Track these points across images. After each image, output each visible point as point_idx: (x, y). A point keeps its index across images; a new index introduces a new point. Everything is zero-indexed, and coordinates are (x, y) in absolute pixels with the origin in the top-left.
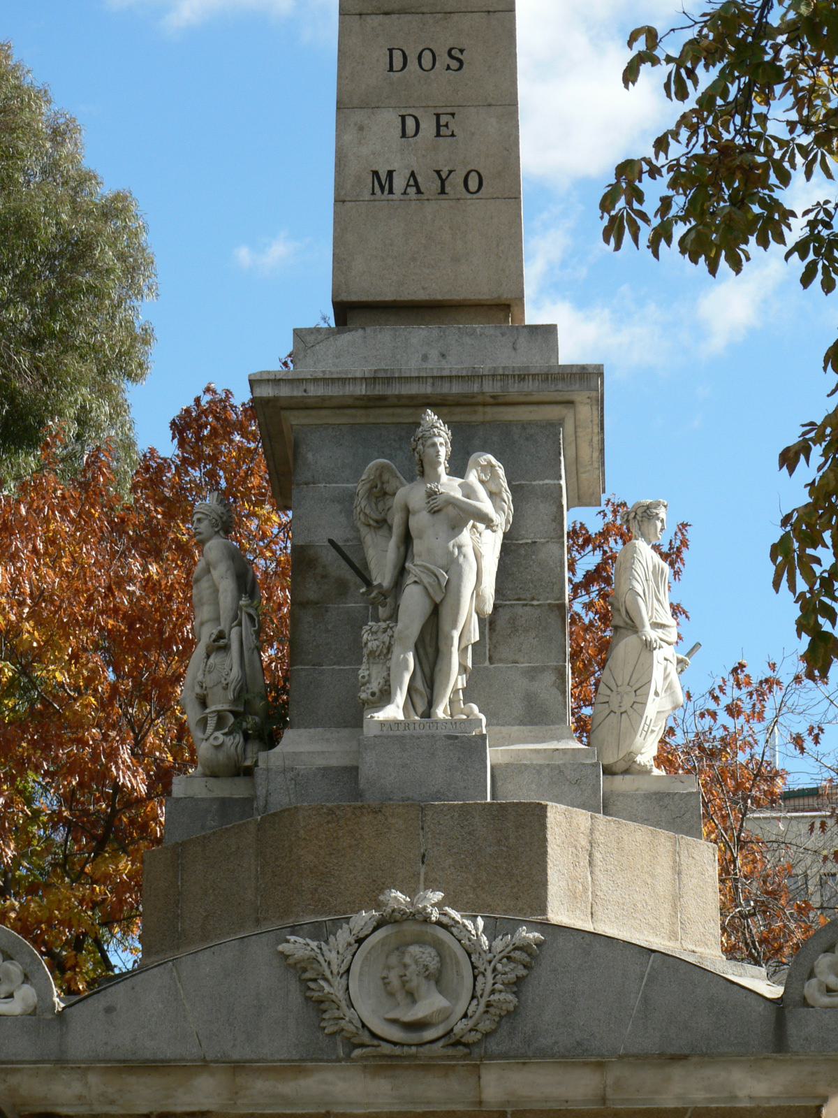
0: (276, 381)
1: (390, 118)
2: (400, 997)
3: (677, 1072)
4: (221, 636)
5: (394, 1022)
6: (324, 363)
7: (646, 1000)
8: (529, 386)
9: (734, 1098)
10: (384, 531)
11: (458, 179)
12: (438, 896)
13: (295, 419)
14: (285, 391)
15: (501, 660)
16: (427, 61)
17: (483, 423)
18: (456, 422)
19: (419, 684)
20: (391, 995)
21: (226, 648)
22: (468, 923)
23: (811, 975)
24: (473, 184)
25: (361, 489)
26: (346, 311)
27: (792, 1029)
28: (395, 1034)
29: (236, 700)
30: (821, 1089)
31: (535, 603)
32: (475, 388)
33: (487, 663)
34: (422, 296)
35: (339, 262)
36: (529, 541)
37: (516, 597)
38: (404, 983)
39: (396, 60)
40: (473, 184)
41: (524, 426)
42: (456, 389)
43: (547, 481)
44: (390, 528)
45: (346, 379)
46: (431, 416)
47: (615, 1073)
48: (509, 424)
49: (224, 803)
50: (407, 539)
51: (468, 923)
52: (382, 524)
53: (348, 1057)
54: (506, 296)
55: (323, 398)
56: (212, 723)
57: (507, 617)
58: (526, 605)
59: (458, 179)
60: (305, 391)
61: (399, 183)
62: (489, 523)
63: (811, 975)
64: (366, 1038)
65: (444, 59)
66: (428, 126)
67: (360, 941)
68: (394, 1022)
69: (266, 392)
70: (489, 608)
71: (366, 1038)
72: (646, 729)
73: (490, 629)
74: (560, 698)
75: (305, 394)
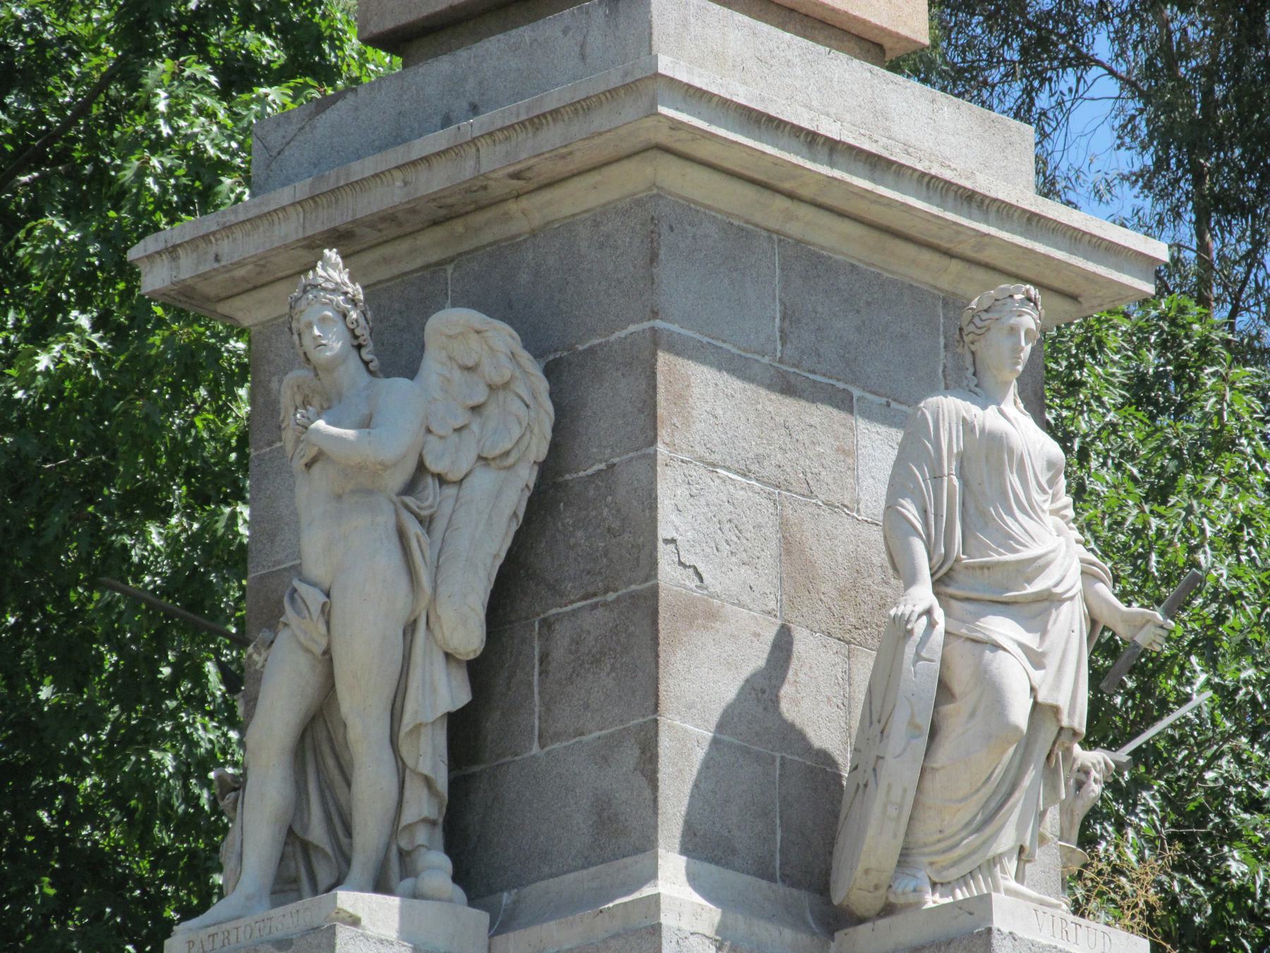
8: (552, 136)
15: (557, 736)
17: (534, 234)
18: (490, 244)
31: (611, 596)
32: (466, 170)
33: (535, 749)
36: (603, 466)
37: (582, 592)
41: (596, 218)
43: (632, 328)
45: (269, 213)
48: (569, 224)
55: (261, 262)
57: (566, 642)
58: (594, 607)
60: (217, 259)
72: (892, 812)
73: (540, 674)
74: (647, 793)
75: (216, 265)
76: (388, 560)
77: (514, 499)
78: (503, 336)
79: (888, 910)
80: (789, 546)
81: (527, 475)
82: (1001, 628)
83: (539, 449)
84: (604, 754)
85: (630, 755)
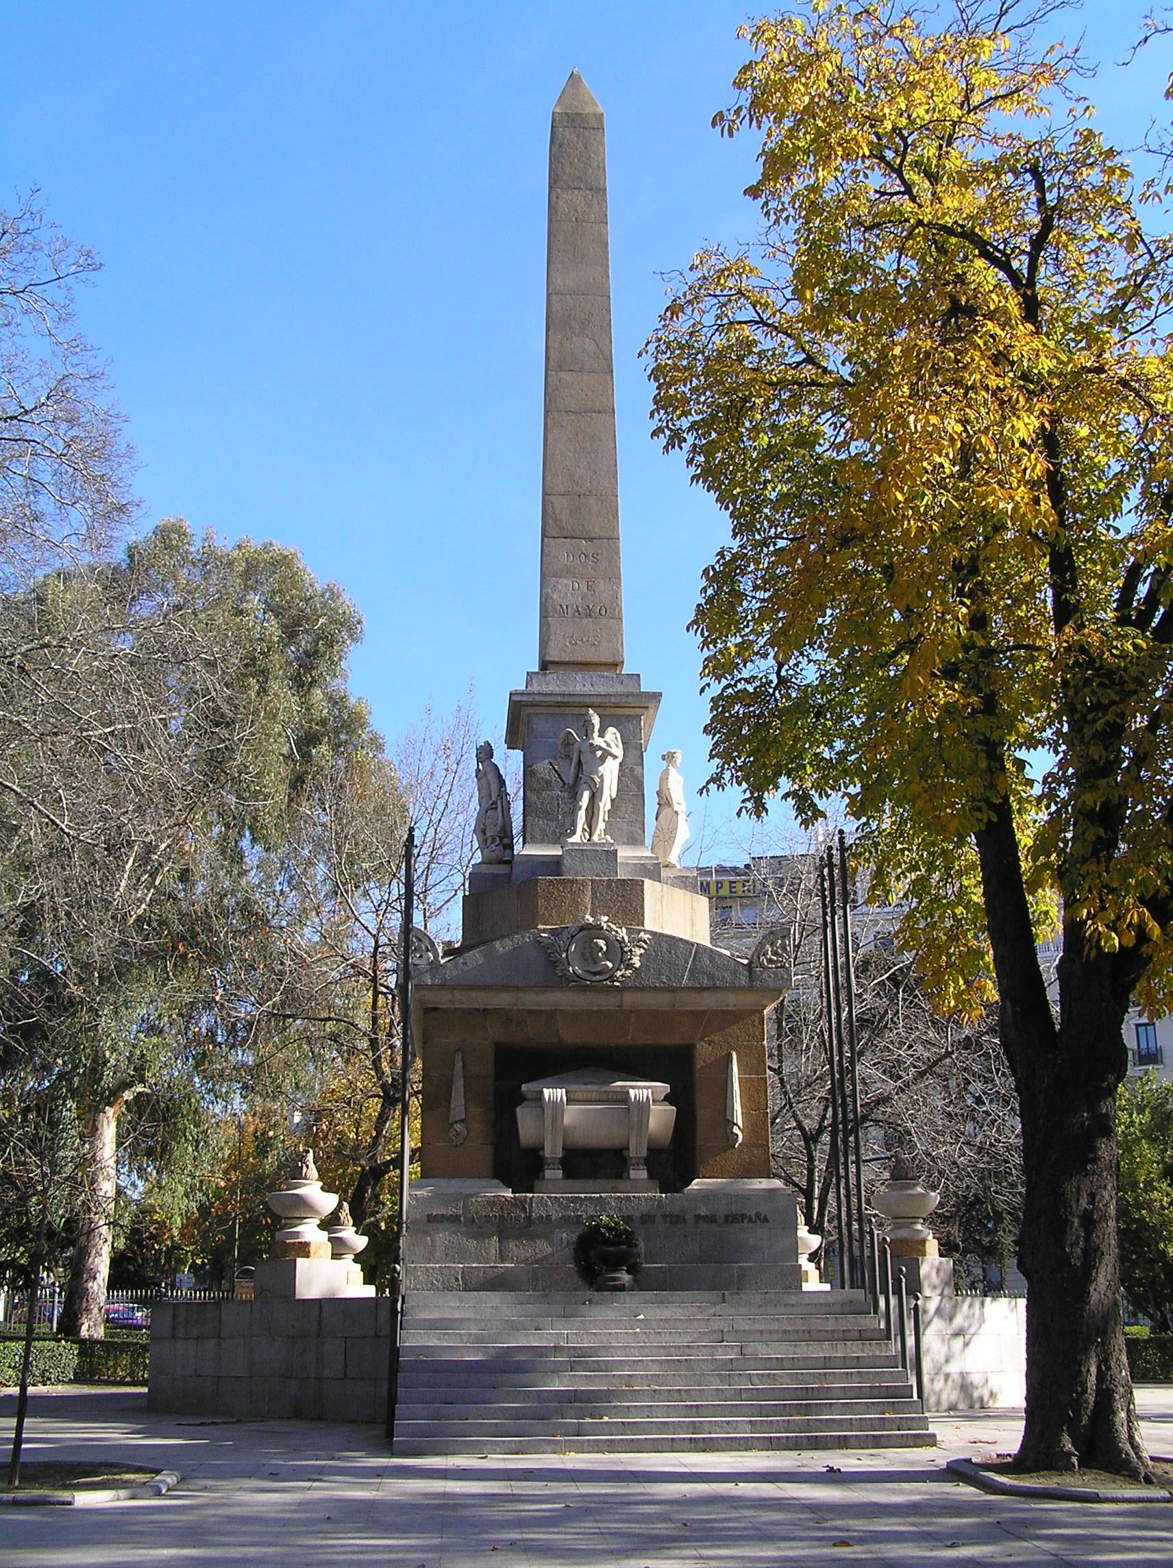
0: (522, 694)
2: (590, 961)
3: (706, 994)
4: (493, 803)
5: (588, 971)
6: (535, 688)
8: (630, 699)
10: (568, 760)
12: (605, 918)
13: (529, 710)
14: (524, 698)
19: (586, 827)
20: (586, 960)
21: (496, 808)
22: (619, 930)
25: (560, 742)
26: (545, 665)
28: (586, 976)
29: (499, 832)
30: (765, 1003)
34: (579, 659)
35: (544, 643)
38: (591, 955)
42: (599, 700)
44: (571, 759)
46: (591, 712)
47: (679, 995)
49: (494, 875)
50: (580, 763)
51: (619, 930)
52: (568, 757)
54: (618, 660)
56: (489, 840)
62: (615, 757)
64: (576, 979)
67: (573, 937)
68: (588, 971)
69: (515, 698)
70: (614, 796)
71: (576, 979)
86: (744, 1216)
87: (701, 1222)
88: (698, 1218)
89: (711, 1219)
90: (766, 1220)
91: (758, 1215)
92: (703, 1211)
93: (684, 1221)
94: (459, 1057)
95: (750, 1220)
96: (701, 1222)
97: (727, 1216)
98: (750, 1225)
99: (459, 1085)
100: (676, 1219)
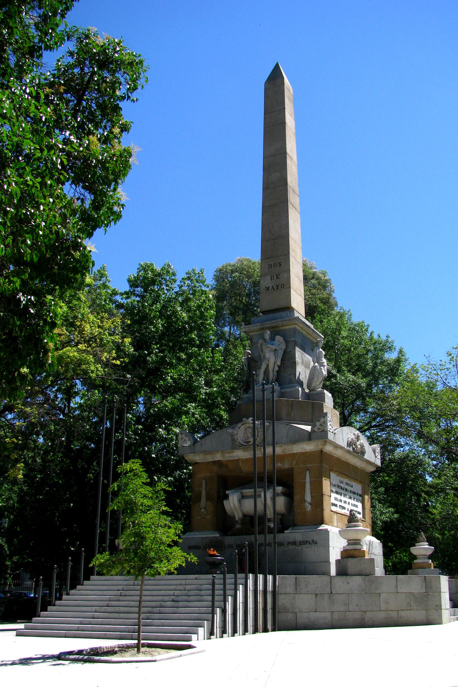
1: (269, 277)
7: (287, 434)
9: (306, 450)
11: (280, 286)
16: (275, 266)
23: (316, 426)
24: (283, 287)
27: (312, 436)
28: (245, 444)
32: (278, 324)
39: (270, 266)
40: (283, 287)
41: (289, 329)
53: (238, 449)
59: (280, 286)
61: (270, 288)
63: (316, 426)
64: (241, 445)
65: (278, 265)
66: (275, 277)
71: (241, 445)
76: (274, 357)
77: (282, 353)
78: (282, 338)
79: (313, 390)
80: (302, 359)
81: (283, 350)
82: (322, 368)
83: (284, 348)
84: (290, 375)
85: (293, 375)
86: (307, 542)
87: (290, 545)
88: (289, 543)
89: (294, 543)
90: (316, 543)
91: (313, 541)
92: (292, 540)
93: (283, 545)
94: (204, 481)
95: (310, 543)
96: (290, 545)
97: (300, 542)
98: (310, 545)
99: (204, 493)
100: (281, 544)
